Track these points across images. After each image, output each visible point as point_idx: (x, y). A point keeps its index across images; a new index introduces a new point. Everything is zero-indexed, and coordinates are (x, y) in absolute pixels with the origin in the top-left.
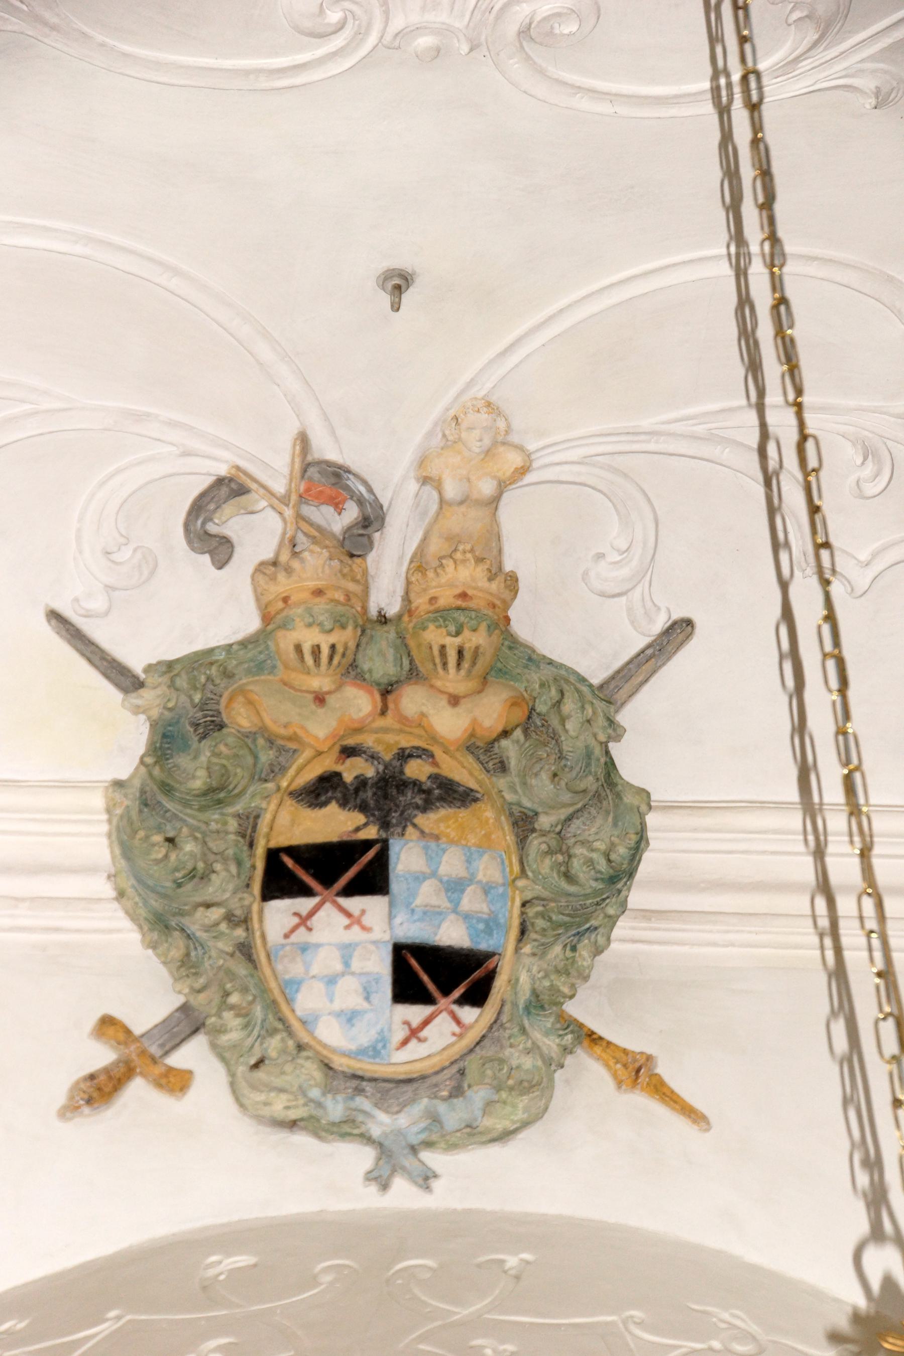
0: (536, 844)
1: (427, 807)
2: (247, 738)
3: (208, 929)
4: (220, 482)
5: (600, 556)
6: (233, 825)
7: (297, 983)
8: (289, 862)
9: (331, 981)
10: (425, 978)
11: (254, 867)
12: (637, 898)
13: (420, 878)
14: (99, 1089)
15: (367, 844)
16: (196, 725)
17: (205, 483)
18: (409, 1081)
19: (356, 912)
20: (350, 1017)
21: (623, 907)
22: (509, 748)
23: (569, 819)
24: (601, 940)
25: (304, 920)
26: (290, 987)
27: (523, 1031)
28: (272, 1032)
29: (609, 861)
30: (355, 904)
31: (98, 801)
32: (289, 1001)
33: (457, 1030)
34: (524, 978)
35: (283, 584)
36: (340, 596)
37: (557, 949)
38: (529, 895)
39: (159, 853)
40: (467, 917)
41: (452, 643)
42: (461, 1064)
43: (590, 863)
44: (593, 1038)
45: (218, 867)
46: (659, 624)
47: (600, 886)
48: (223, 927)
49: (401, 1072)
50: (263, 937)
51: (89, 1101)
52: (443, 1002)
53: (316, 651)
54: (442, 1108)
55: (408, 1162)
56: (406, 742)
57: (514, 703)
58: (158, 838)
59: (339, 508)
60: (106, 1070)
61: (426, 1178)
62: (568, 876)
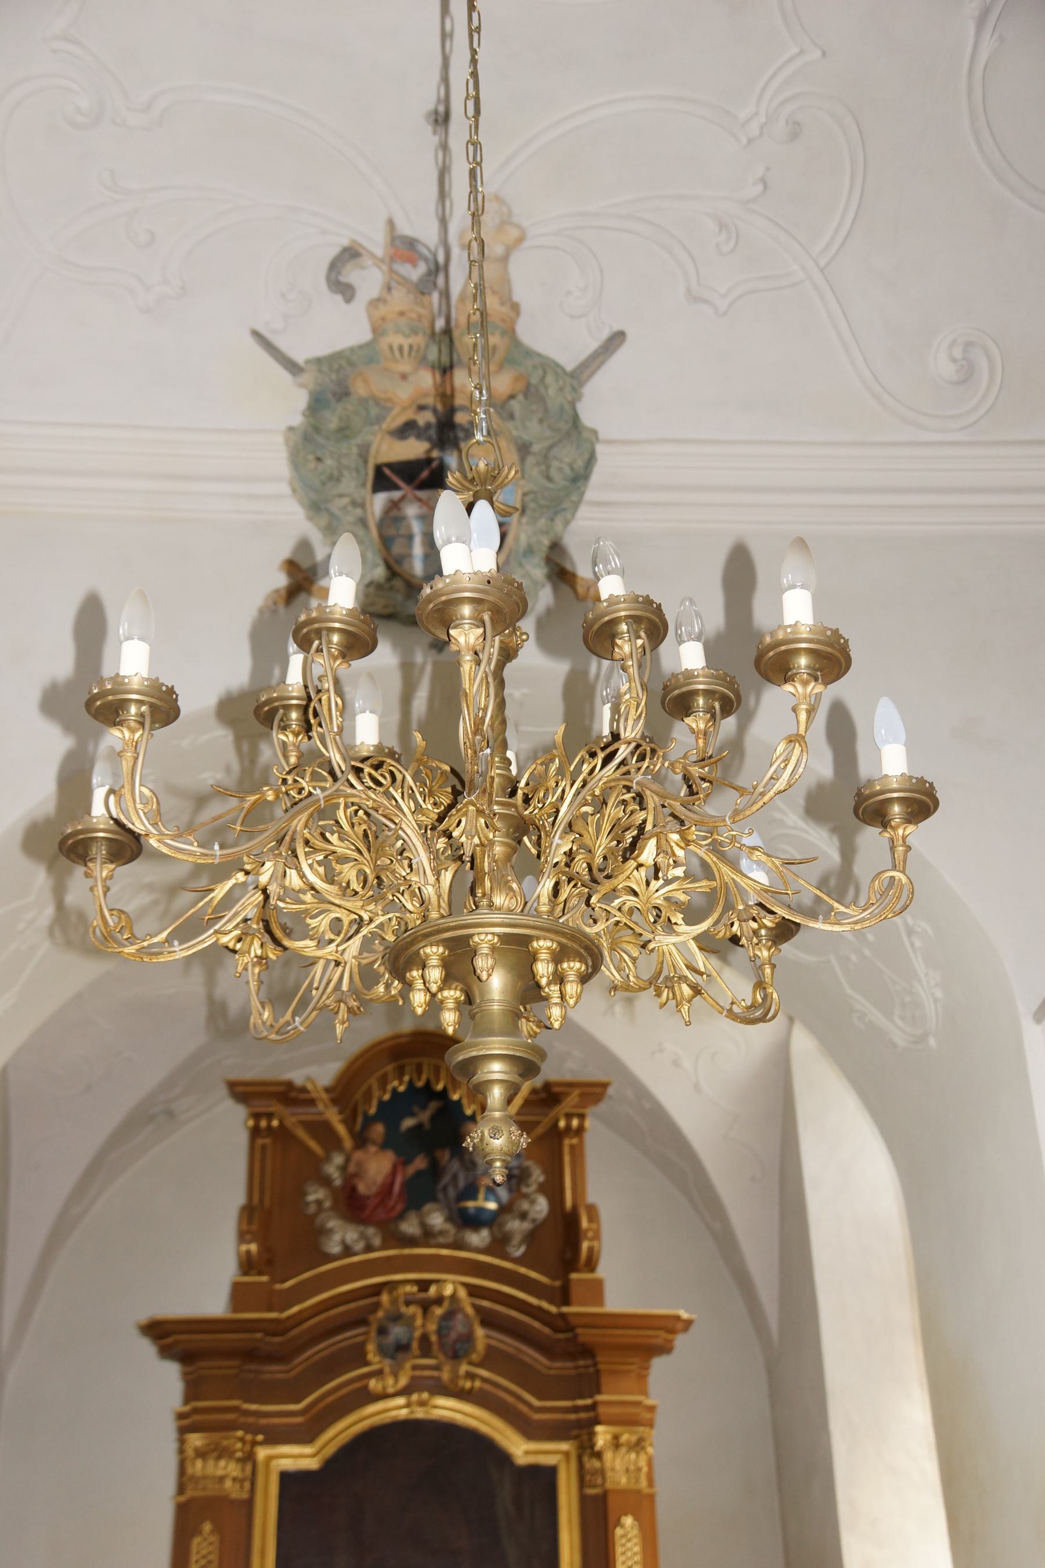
0: (530, 460)
2: (363, 401)
3: (344, 508)
5: (569, 293)
6: (355, 450)
8: (387, 471)
11: (366, 474)
16: (334, 394)
21: (582, 494)
22: (516, 406)
23: (551, 447)
24: (569, 516)
27: (521, 565)
29: (572, 469)
31: (280, 439)
34: (523, 537)
35: (383, 310)
38: (526, 489)
39: (312, 465)
43: (560, 470)
46: (605, 334)
47: (566, 483)
48: (350, 508)
53: (401, 349)
57: (517, 379)
58: (311, 457)
59: (414, 265)
62: (549, 478)
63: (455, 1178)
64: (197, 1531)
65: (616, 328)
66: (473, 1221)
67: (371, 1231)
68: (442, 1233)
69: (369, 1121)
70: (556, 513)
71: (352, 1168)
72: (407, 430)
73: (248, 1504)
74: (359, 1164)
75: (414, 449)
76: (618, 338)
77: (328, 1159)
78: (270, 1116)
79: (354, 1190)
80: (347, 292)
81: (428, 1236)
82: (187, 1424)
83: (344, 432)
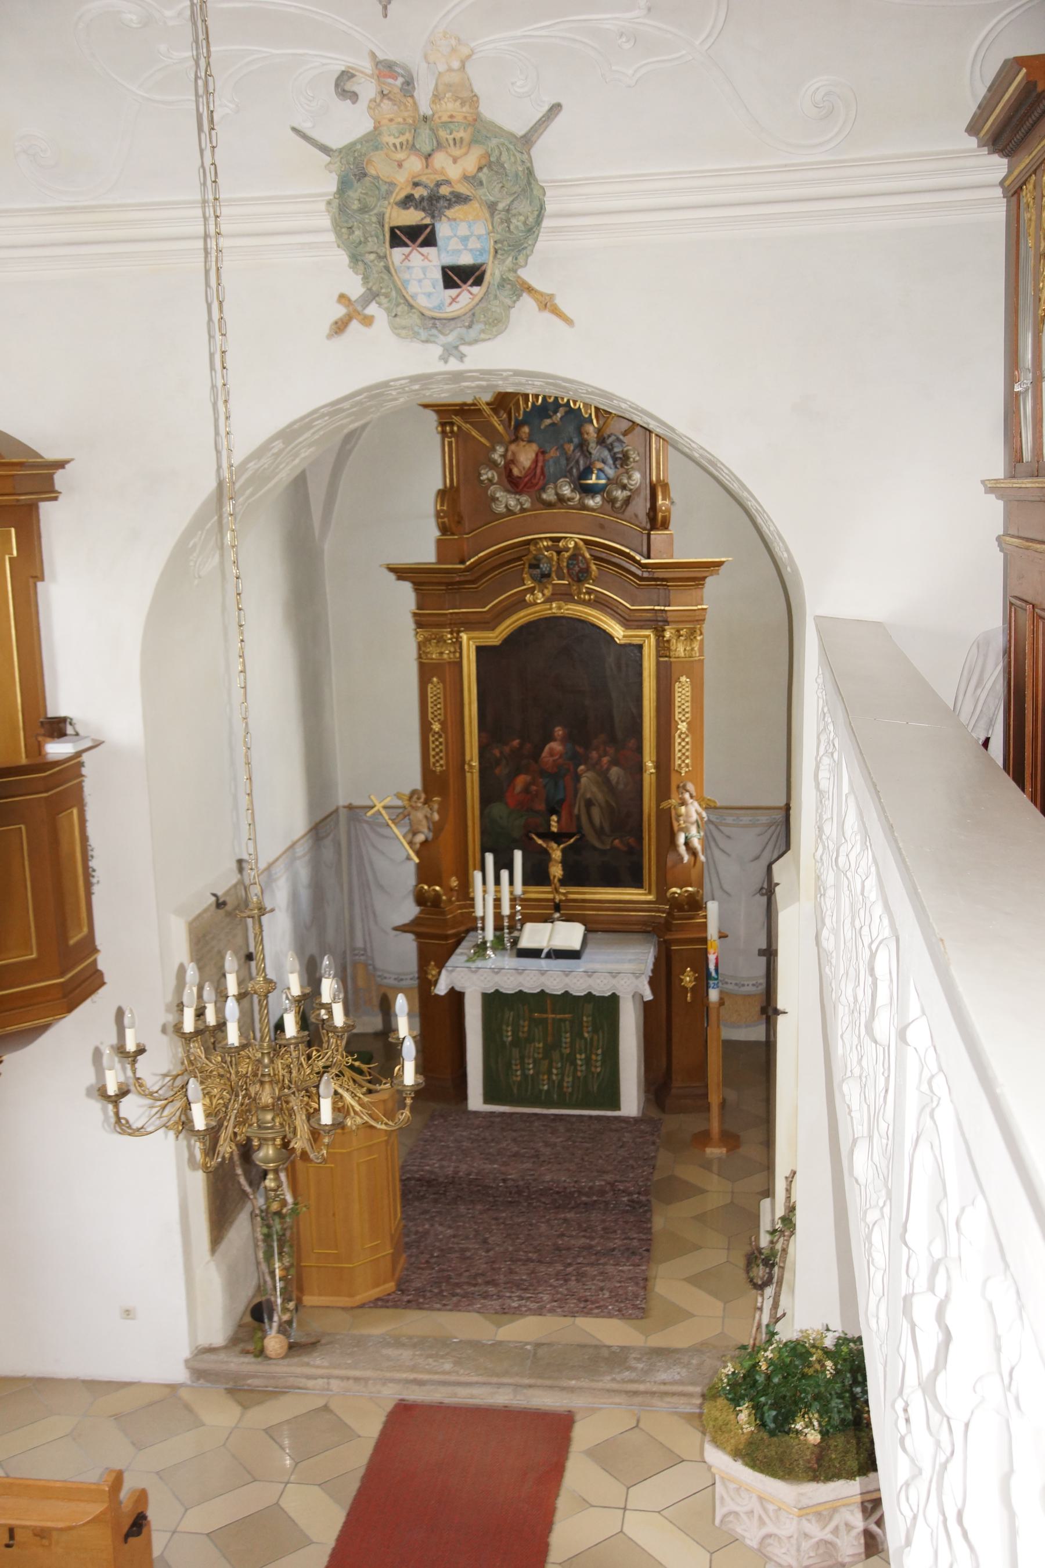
0: (497, 218)
1: (449, 207)
3: (372, 261)
4: (343, 72)
6: (374, 219)
7: (408, 281)
8: (398, 232)
9: (420, 281)
10: (456, 278)
12: (546, 223)
13: (449, 238)
14: (339, 329)
15: (426, 226)
16: (355, 175)
17: (338, 73)
18: (453, 319)
19: (425, 254)
20: (429, 295)
22: (483, 176)
25: (407, 257)
26: (405, 283)
27: (496, 297)
28: (398, 305)
30: (425, 250)
32: (405, 289)
33: (471, 296)
34: (497, 272)
36: (400, 120)
37: (510, 259)
40: (471, 250)
41: (450, 137)
42: (473, 311)
44: (530, 289)
45: (370, 239)
46: (546, 108)
49: (450, 315)
50: (393, 262)
51: (336, 333)
52: (464, 287)
53: (394, 145)
54: (464, 330)
55: (455, 352)
56: (439, 178)
57: (482, 157)
59: (395, 78)
60: (341, 319)
61: (461, 358)
63: (577, 462)
64: (430, 681)
65: (554, 101)
66: (589, 491)
67: (524, 498)
68: (570, 499)
69: (519, 425)
70: (519, 251)
71: (509, 455)
72: (408, 201)
73: (459, 664)
74: (514, 454)
75: (413, 217)
76: (555, 109)
77: (494, 450)
78: (452, 424)
79: (511, 471)
80: (354, 97)
81: (561, 499)
82: (421, 622)
83: (364, 209)
